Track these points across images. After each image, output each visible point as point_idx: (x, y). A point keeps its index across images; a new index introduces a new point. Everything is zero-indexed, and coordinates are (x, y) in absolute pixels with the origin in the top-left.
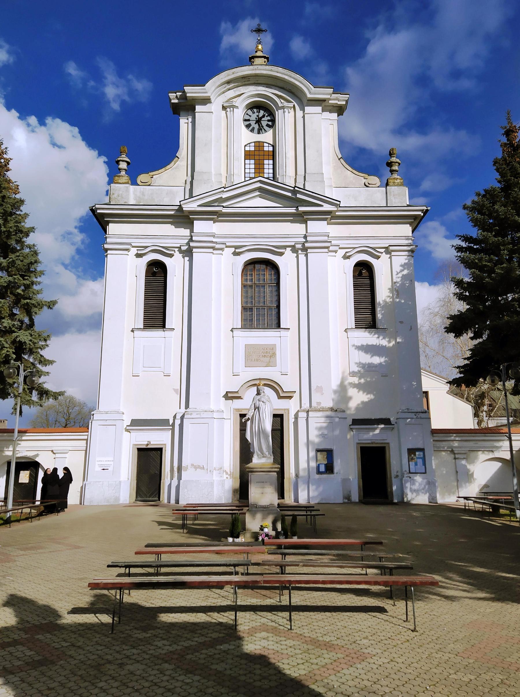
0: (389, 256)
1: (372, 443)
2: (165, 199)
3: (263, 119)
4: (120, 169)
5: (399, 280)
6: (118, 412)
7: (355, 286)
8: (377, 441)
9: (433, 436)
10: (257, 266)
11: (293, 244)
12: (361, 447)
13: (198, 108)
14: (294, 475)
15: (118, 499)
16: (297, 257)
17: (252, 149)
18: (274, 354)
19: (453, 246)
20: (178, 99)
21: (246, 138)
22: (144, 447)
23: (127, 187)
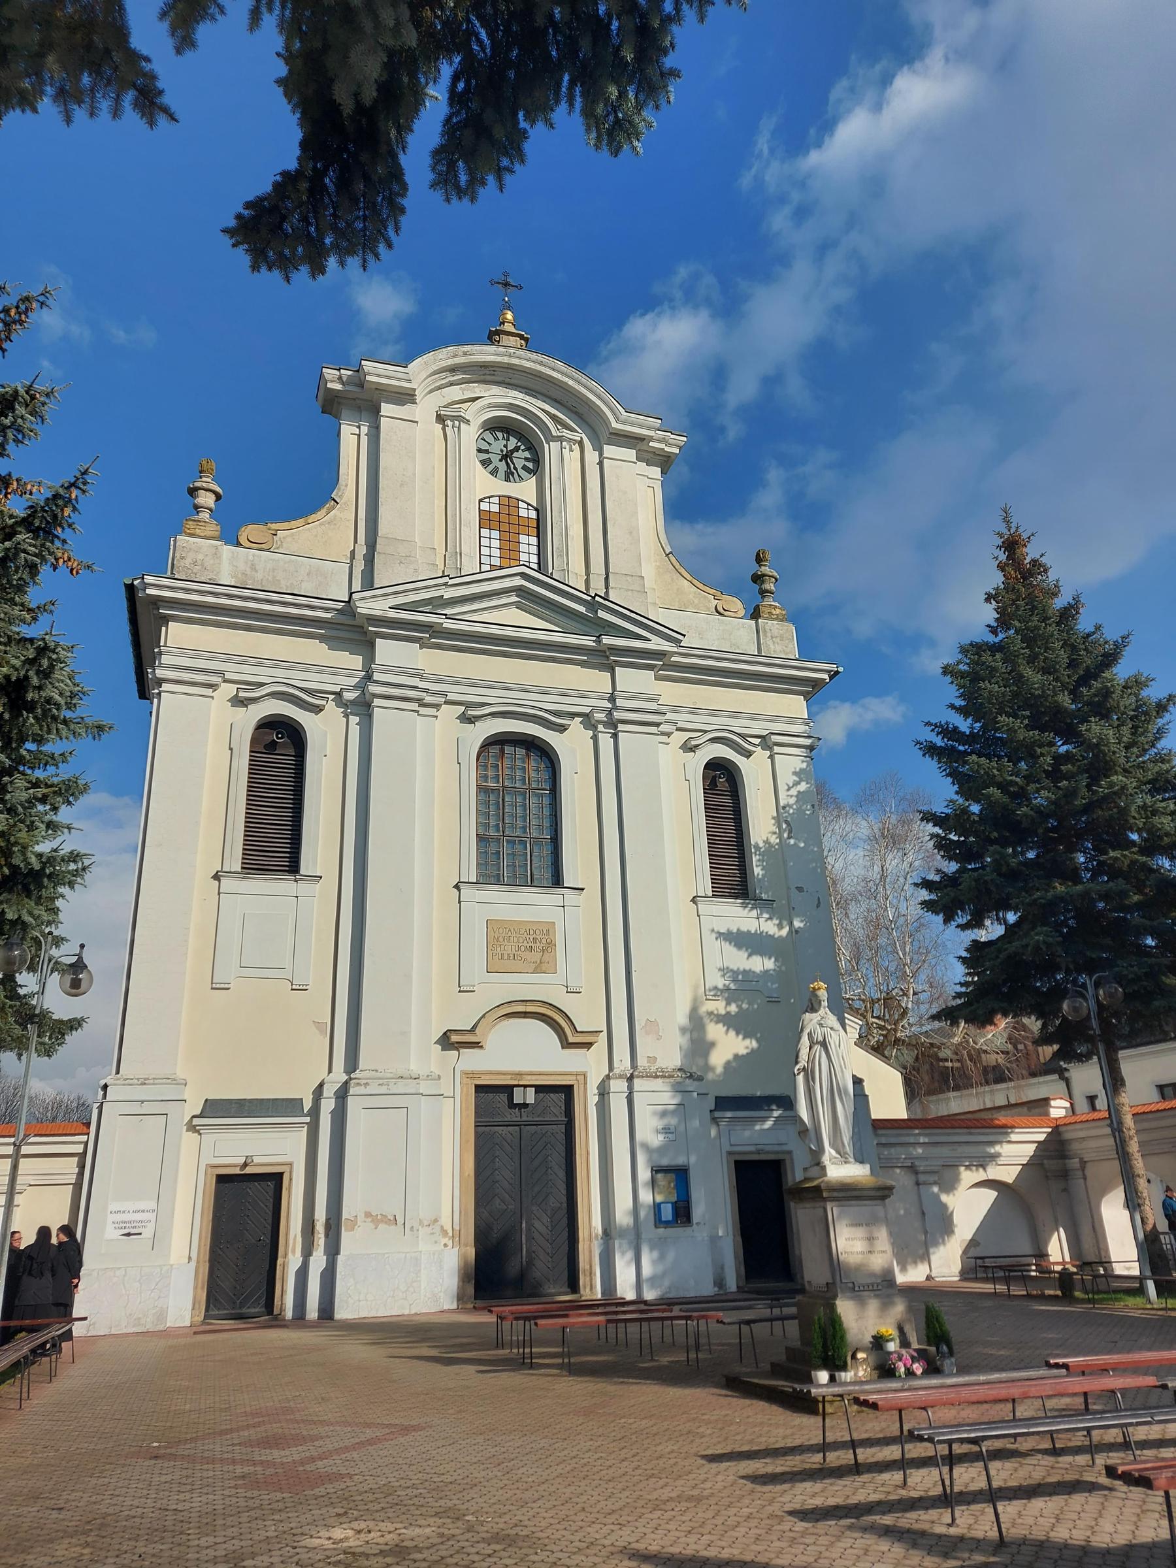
0: (768, 753)
1: (758, 1152)
2: (304, 585)
3: (515, 454)
4: (196, 507)
5: (792, 801)
6: (173, 1081)
7: (707, 808)
8: (768, 1148)
9: (876, 1135)
10: (508, 749)
11: (587, 710)
12: (736, 1162)
13: (386, 409)
14: (600, 1232)
15: (162, 1315)
16: (595, 739)
17: (495, 508)
18: (551, 945)
19: (918, 743)
20: (343, 384)
21: (482, 485)
22: (237, 1171)
23: (216, 548)
